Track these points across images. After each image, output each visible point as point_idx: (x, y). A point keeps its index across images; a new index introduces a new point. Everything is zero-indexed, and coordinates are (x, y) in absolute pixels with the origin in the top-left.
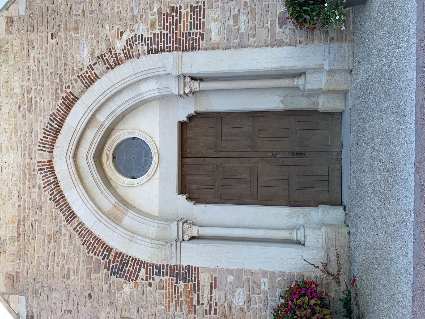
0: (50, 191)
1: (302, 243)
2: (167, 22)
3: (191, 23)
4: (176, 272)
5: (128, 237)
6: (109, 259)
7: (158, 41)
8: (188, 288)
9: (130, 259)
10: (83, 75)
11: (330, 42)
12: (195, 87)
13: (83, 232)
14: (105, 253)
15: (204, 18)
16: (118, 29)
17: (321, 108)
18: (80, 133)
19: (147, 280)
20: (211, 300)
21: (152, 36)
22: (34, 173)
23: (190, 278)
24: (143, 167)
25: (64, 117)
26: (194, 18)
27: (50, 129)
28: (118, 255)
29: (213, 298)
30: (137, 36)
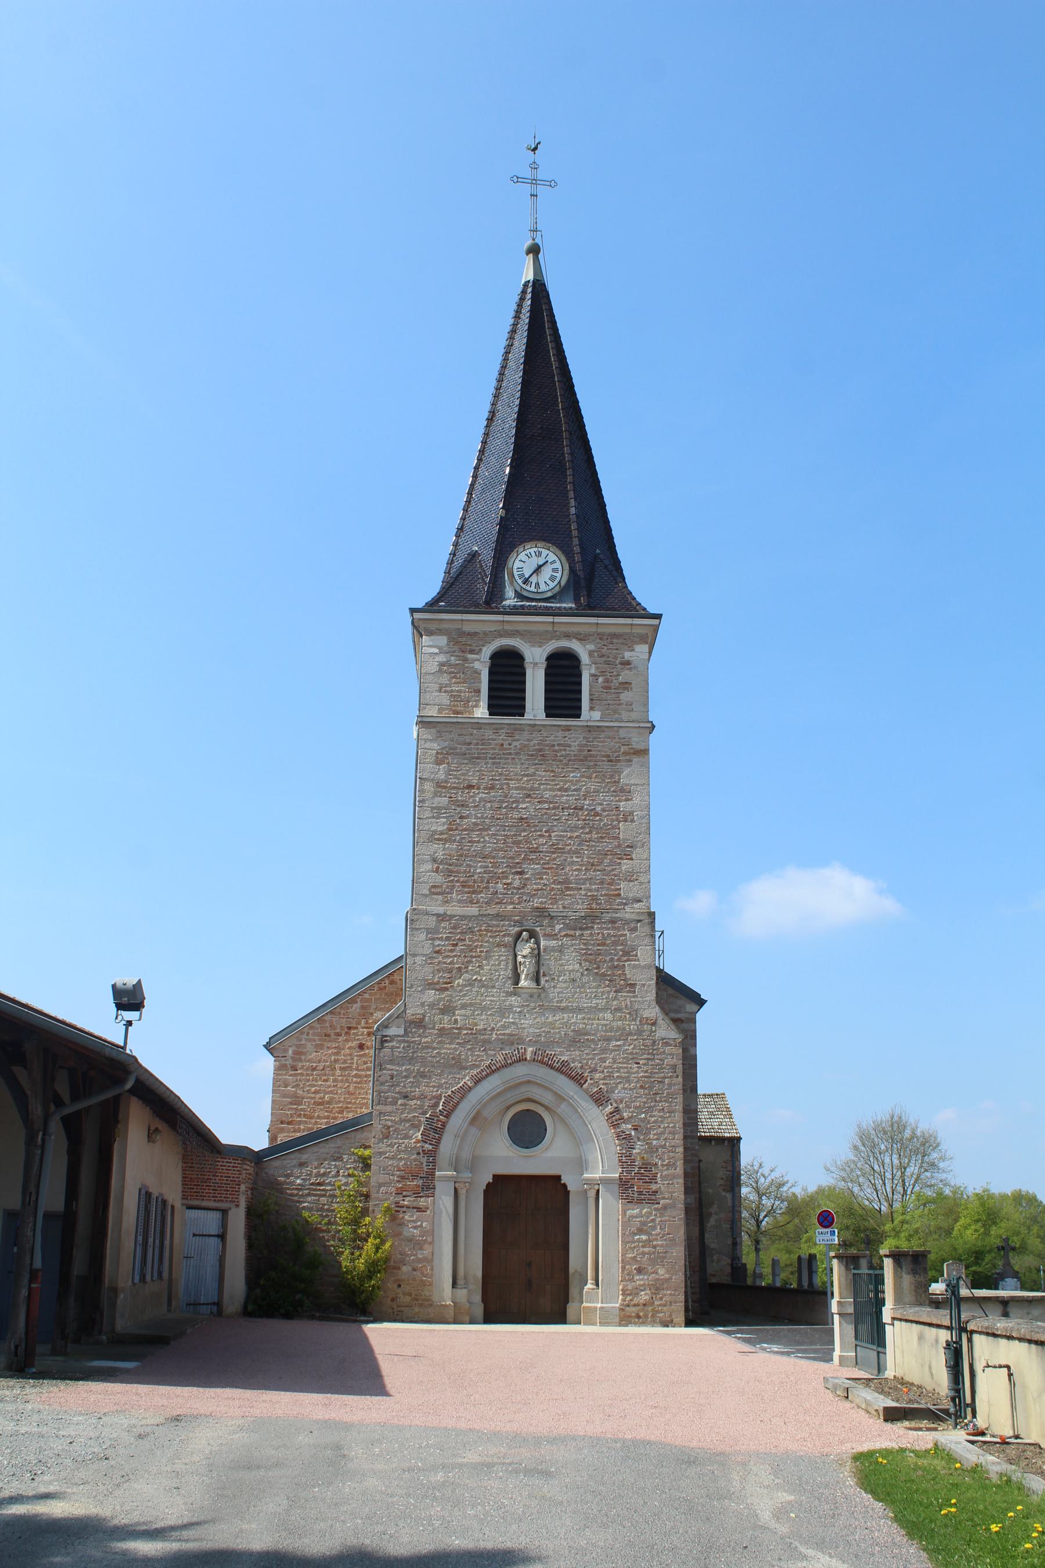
20: (407, 1207)
21: (632, 1158)
28: (444, 1125)
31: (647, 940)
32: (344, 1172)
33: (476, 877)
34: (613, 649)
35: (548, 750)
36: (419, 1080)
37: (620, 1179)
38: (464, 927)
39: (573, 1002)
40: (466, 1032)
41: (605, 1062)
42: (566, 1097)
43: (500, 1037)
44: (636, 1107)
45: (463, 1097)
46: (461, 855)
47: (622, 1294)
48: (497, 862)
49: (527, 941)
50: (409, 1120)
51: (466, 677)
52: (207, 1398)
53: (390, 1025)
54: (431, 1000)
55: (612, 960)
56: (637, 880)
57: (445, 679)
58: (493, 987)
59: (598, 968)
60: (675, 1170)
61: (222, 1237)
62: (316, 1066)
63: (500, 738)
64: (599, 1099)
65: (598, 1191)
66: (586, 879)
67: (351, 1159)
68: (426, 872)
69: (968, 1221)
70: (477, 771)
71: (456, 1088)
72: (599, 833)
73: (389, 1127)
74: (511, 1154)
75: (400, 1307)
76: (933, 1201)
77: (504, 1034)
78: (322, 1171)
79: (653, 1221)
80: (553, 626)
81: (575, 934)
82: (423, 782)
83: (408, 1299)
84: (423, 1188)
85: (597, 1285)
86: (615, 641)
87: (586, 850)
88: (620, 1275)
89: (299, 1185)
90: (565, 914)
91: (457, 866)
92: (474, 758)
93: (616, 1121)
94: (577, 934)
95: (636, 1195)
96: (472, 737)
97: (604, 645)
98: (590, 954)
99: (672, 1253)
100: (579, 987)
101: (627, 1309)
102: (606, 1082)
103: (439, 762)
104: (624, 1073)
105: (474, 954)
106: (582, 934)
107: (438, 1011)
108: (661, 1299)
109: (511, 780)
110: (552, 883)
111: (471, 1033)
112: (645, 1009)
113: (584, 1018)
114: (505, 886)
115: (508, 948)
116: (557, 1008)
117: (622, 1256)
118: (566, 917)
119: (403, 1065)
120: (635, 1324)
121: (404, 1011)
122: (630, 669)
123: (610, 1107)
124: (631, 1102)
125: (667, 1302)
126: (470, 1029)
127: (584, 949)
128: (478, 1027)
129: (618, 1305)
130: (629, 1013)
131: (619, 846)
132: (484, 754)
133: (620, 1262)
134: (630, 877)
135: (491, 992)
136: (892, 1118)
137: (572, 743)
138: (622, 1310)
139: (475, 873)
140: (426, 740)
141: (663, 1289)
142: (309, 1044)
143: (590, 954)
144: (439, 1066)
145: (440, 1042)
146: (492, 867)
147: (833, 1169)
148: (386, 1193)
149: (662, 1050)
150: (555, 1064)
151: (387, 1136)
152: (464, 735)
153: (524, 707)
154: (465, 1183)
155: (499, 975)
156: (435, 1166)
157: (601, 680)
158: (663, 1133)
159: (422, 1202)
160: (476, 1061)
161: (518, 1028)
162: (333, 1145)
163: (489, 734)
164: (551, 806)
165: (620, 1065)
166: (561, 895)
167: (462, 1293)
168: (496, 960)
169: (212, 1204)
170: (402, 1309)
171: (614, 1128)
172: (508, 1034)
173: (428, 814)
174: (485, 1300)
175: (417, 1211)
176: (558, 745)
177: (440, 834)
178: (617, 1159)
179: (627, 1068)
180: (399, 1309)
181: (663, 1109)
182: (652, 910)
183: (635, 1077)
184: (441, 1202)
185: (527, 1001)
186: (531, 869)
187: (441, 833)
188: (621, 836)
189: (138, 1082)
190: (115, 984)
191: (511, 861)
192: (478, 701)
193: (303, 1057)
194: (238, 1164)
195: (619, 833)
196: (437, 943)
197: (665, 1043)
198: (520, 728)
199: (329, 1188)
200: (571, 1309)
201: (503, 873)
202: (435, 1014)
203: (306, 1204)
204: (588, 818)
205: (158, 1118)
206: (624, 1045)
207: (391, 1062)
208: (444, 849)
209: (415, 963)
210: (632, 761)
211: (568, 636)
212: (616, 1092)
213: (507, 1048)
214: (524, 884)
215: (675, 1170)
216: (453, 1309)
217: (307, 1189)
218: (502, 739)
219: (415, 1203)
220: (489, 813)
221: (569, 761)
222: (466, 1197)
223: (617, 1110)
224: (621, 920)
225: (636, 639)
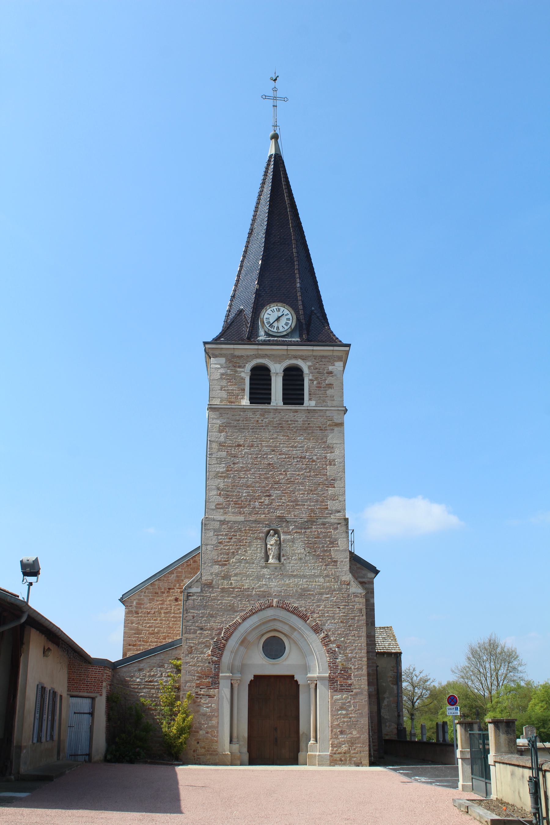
1: (232, 743)
3: (343, 685)
9: (222, 652)
15: (345, 691)
16: (341, 645)
18: (288, 623)
21: (337, 664)
27: (290, 607)
28: (224, 645)
29: (204, 697)
31: (344, 535)
32: (165, 674)
33: (243, 498)
34: (322, 365)
35: (285, 424)
36: (209, 619)
38: (236, 528)
39: (300, 572)
40: (237, 590)
41: (320, 607)
42: (297, 628)
43: (258, 593)
44: (338, 634)
46: (234, 486)
47: (331, 747)
48: (255, 490)
49: (273, 536)
50: (204, 643)
51: (237, 381)
52: (66, 816)
53: (192, 586)
54: (217, 571)
55: (323, 547)
56: (337, 499)
57: (224, 383)
58: (253, 563)
59: (315, 551)
60: (362, 671)
61: (92, 714)
62: (150, 611)
63: (257, 417)
64: (317, 629)
65: (316, 684)
66: (308, 499)
67: (169, 666)
68: (213, 496)
69: (537, 701)
70: (243, 436)
71: (232, 623)
72: (315, 472)
73: (192, 647)
74: (264, 663)
75: (198, 755)
76: (514, 690)
77: (260, 591)
78: (152, 673)
79: (349, 702)
80: (287, 352)
81: (301, 531)
82: (211, 443)
83: (203, 751)
84: (212, 684)
85: (316, 741)
86: (323, 360)
87: (308, 482)
88: (330, 735)
89: (138, 682)
90: (295, 520)
91: (231, 492)
92: (241, 429)
93: (327, 642)
94: (303, 532)
95: (339, 687)
96: (240, 417)
97: (317, 362)
98: (311, 544)
99: (361, 721)
100: (304, 563)
101: (335, 755)
102: (320, 619)
103: (220, 431)
105: (242, 544)
106: (306, 532)
107: (220, 578)
108: (355, 749)
109: (263, 441)
110: (288, 502)
111: (241, 591)
112: (343, 576)
113: (307, 581)
114: (260, 504)
115: (262, 540)
116: (291, 575)
117: (331, 723)
118: (296, 521)
119: (200, 610)
120: (339, 765)
121: (201, 578)
122: (332, 376)
123: (323, 634)
125: (358, 751)
126: (240, 588)
127: (307, 541)
128: (244, 587)
129: (329, 753)
130: (334, 578)
131: (327, 479)
132: (247, 426)
133: (330, 727)
134: (334, 498)
135: (252, 566)
136: (490, 641)
137: (299, 420)
138: (331, 756)
139: (242, 496)
140: (213, 419)
141: (356, 744)
142: (145, 599)
143: (311, 544)
144: (221, 611)
145: (222, 596)
146: (252, 493)
147: (456, 671)
148: (190, 687)
149: (353, 600)
150: (290, 609)
151: (191, 653)
152: (236, 415)
153: (270, 399)
154: (237, 680)
155: (257, 556)
156: (219, 670)
157: (315, 382)
158: (355, 649)
159: (212, 692)
161: (268, 588)
162: (158, 658)
163: (250, 414)
164: (287, 456)
165: (329, 609)
166: (293, 508)
167: (236, 747)
168: (255, 547)
169: (85, 694)
170: (200, 757)
171: (325, 647)
172: (262, 591)
173: (214, 462)
174: (249, 750)
175: (209, 697)
176: (290, 421)
177: (221, 474)
178: (328, 665)
179: (333, 611)
180: (198, 757)
181: (354, 635)
182: (347, 517)
183: (338, 616)
185: (273, 571)
186: (275, 493)
187: (222, 473)
188: (328, 474)
189: (29, 616)
190: (22, 560)
191: (263, 489)
192: (244, 395)
193: (142, 606)
194: (102, 670)
195: (327, 472)
196: (220, 537)
197: (354, 595)
198: (268, 411)
199: (156, 684)
200: (301, 756)
201: (258, 496)
202: (219, 579)
203: (143, 694)
204: (308, 463)
205: (50, 642)
206: (331, 597)
207: (193, 608)
208: (224, 482)
209: (207, 549)
210: (334, 430)
211: (296, 357)
212: (327, 625)
213: (262, 599)
214: (271, 502)
215: (362, 671)
217: (143, 685)
218: (258, 418)
219: (207, 693)
220: (250, 461)
221: (297, 430)
223: (327, 636)
224: (329, 523)
225: (336, 359)
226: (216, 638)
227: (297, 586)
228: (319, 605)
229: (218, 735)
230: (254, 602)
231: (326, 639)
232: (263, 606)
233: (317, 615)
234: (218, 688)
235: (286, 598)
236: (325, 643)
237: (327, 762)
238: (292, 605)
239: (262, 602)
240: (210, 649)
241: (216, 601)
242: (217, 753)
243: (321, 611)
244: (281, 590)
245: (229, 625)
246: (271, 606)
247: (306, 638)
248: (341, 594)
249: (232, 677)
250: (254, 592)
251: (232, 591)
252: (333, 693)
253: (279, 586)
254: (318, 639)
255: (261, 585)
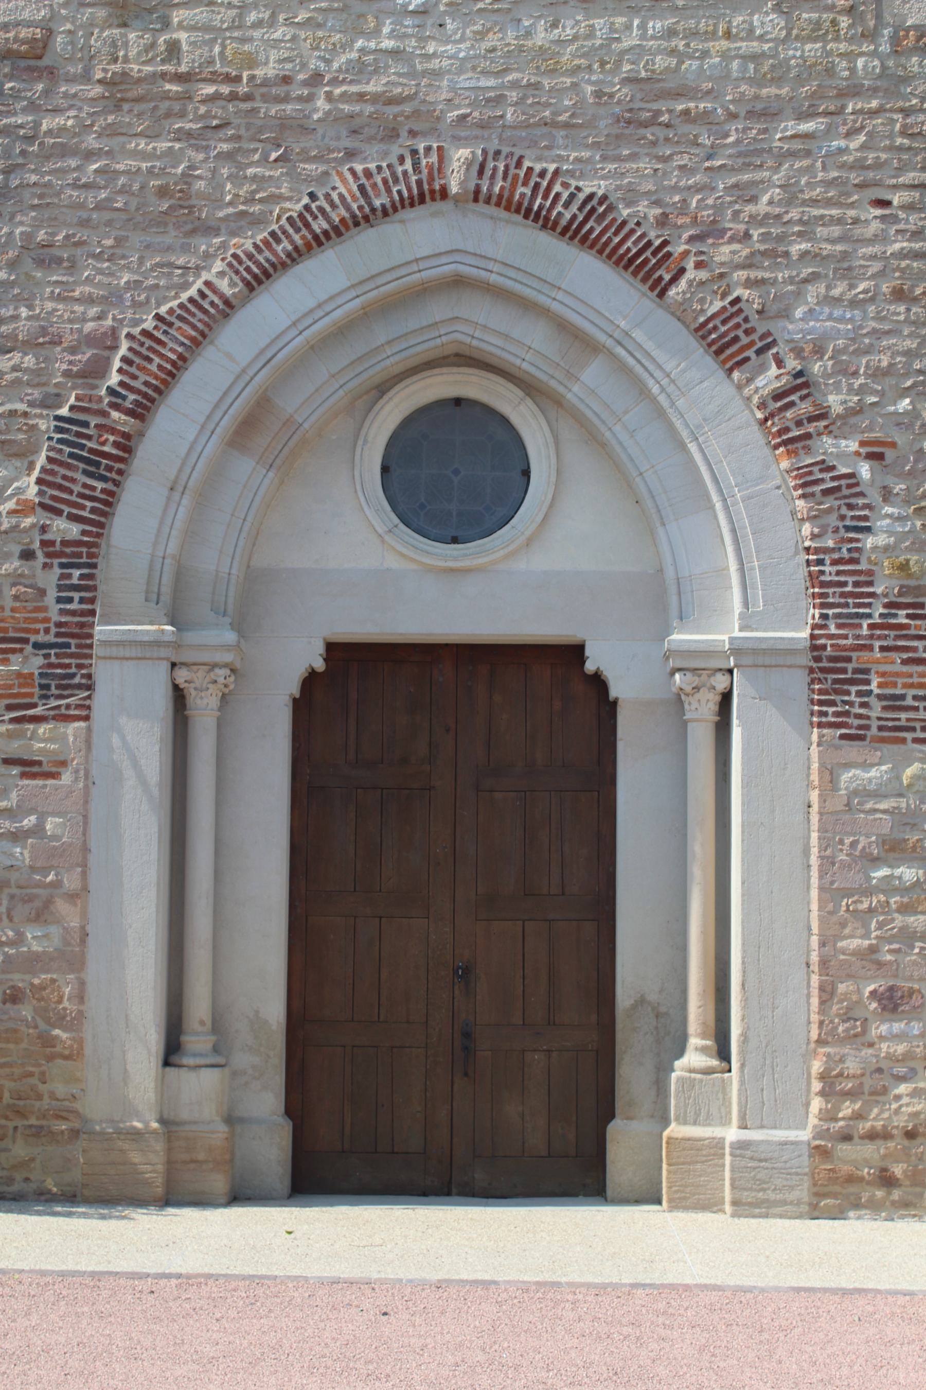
0: (341, 196)
1: (174, 1059)
2: (908, 616)
3: (903, 697)
4: (73, 642)
5: (184, 477)
6: (107, 409)
7: (845, 584)
8: (20, 686)
9: (110, 486)
10: (743, 316)
11: (817, 1147)
12: (695, 705)
13: (200, 315)
14: (132, 397)
15: (916, 740)
16: (893, 445)
17: (615, 1128)
18: (542, 299)
19: (44, 543)
21: (863, 566)
22: (404, 133)
23: (54, 691)
24: (422, 506)
25: (598, 247)
26: (916, 709)
27: (558, 195)
30: (866, 512)
36: (28, 276)
37: (815, 647)
40: (210, 90)
41: (754, 199)
42: (602, 338)
43: (346, 108)
44: (878, 373)
45: (197, 343)
47: (822, 1093)
65: (726, 697)
71: (174, 304)
74: (393, 562)
77: (361, 97)
84: (42, 687)
85: (724, 1053)
88: (815, 1018)
93: (799, 424)
95: (876, 710)
101: (844, 1149)
102: (760, 274)
104: (827, 240)
111: (233, 97)
113: (671, 33)
117: (822, 944)
120: (875, 1207)
123: (773, 371)
124: (859, 352)
126: (229, 79)
129: (804, 1135)
133: (815, 968)
138: (821, 1152)
144: (109, 223)
145: (111, 131)
150: (559, 208)
154: (213, 666)
160: (250, 201)
161: (412, 74)
165: (816, 212)
172: (375, 98)
175: (23, 775)
178: (803, 572)
179: (840, 221)
183: (873, 257)
184: (116, 740)
206: (829, 131)
212: (799, 313)
213: (373, 149)
216: (159, 1146)
219: (16, 744)
222: (220, 724)
226: (72, 401)
227: (603, 64)
228: (753, 183)
229: (80, 1013)
230: (322, 168)
231: (792, 404)
232: (378, 195)
233: (736, 246)
234: (87, 718)
235: (533, 144)
236: (787, 430)
237: (792, 1188)
238: (574, 183)
239: (372, 166)
240: (31, 467)
241: (73, 163)
242: (76, 1125)
243: (761, 224)
244: (502, 86)
245: (158, 317)
246: (432, 192)
247: (662, 399)
248: (898, 116)
249: (177, 646)
250: (321, 104)
251: (179, 97)
252: (837, 748)
253: (483, 64)
254: (738, 402)
255: (370, 58)
